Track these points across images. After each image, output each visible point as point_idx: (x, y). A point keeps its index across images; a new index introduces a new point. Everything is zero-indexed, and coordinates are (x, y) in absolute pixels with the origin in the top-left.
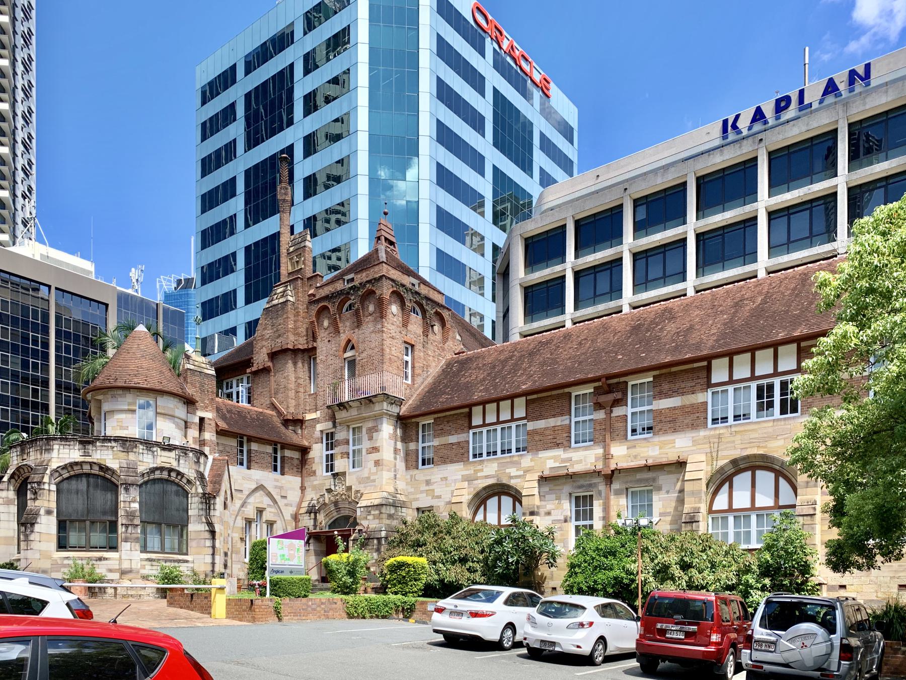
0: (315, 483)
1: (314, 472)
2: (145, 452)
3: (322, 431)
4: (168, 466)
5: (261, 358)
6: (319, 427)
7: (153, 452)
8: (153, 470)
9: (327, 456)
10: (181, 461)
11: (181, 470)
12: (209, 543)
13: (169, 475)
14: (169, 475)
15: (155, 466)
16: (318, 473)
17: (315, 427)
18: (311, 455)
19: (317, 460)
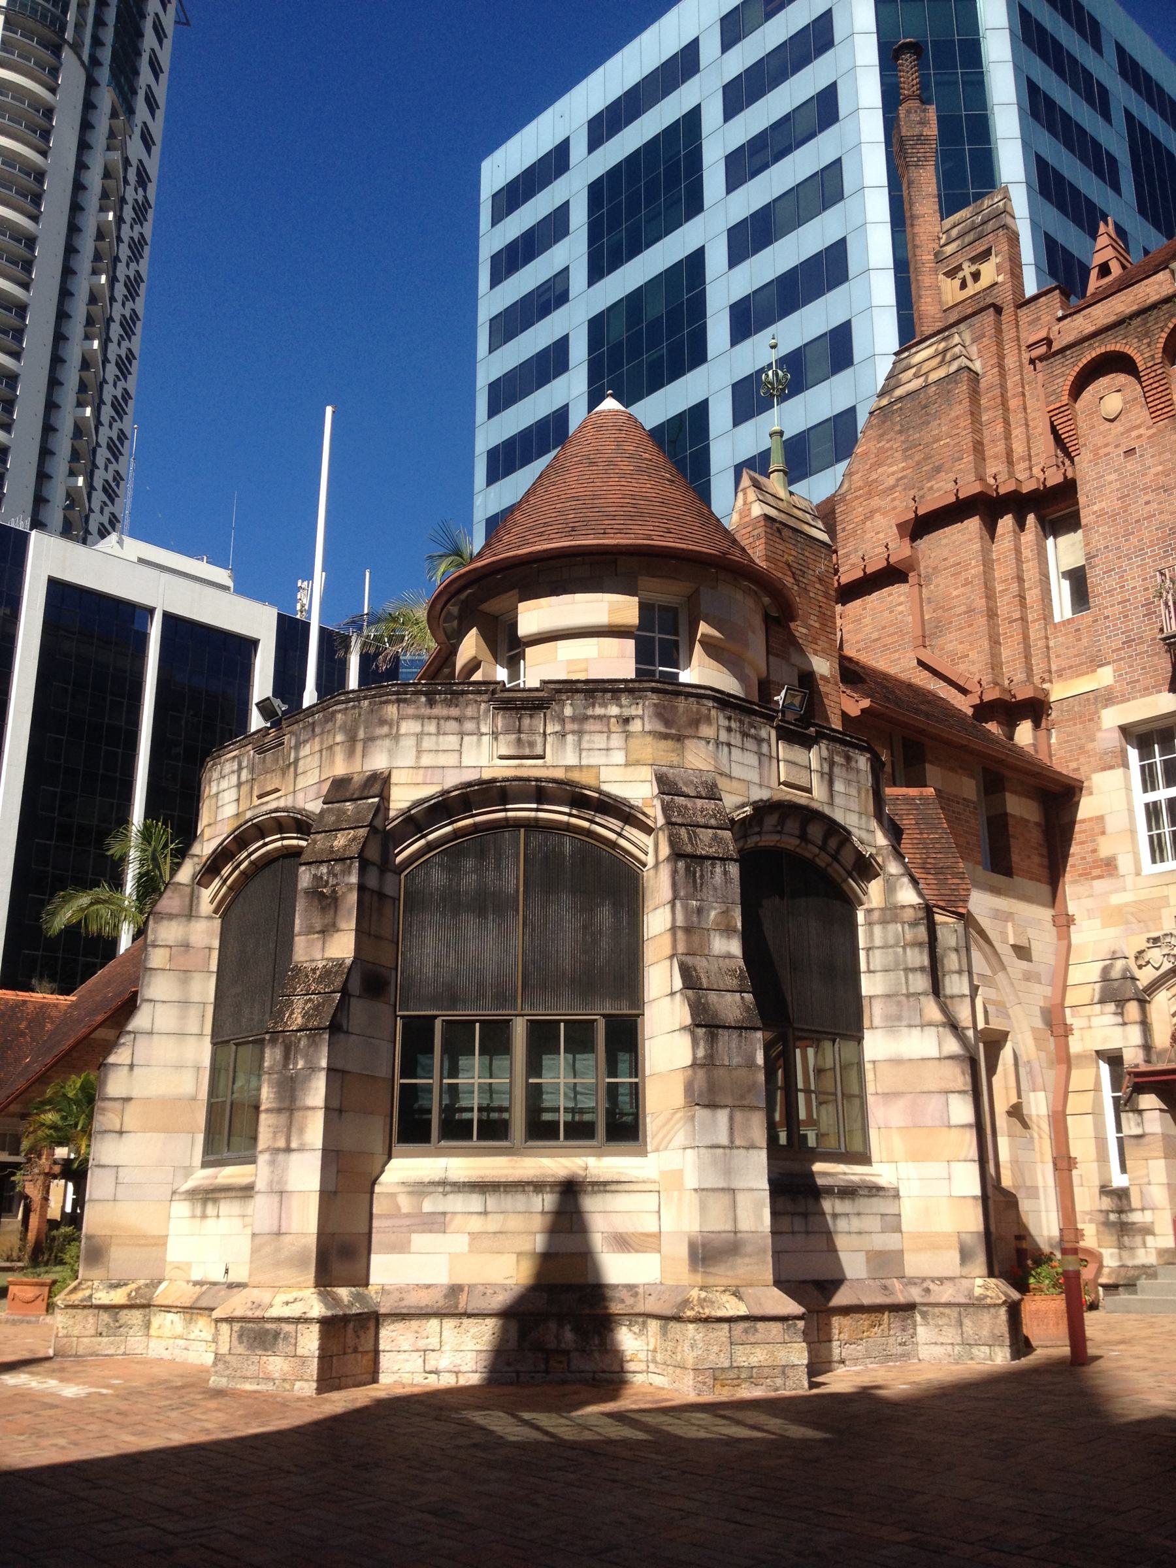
0: (1116, 899)
1: (1109, 866)
2: (736, 739)
3: (1124, 730)
4: (800, 798)
5: (871, 540)
6: (1112, 718)
7: (759, 741)
8: (763, 809)
9: (1152, 811)
10: (839, 786)
11: (838, 816)
12: (962, 1111)
13: (803, 837)
14: (803, 837)
15: (764, 794)
16: (1125, 864)
17: (1093, 718)
18: (1086, 808)
19: (1112, 825)
